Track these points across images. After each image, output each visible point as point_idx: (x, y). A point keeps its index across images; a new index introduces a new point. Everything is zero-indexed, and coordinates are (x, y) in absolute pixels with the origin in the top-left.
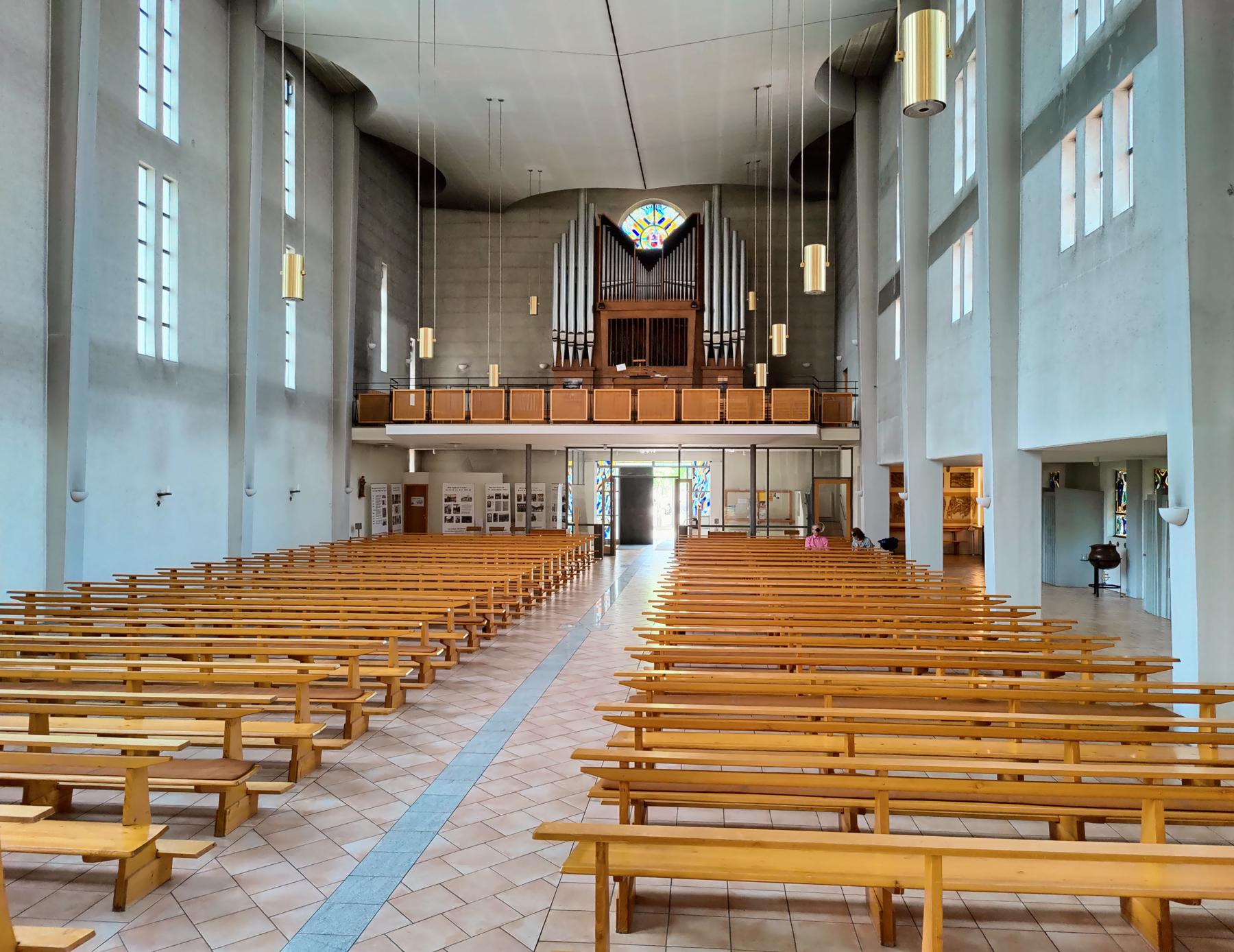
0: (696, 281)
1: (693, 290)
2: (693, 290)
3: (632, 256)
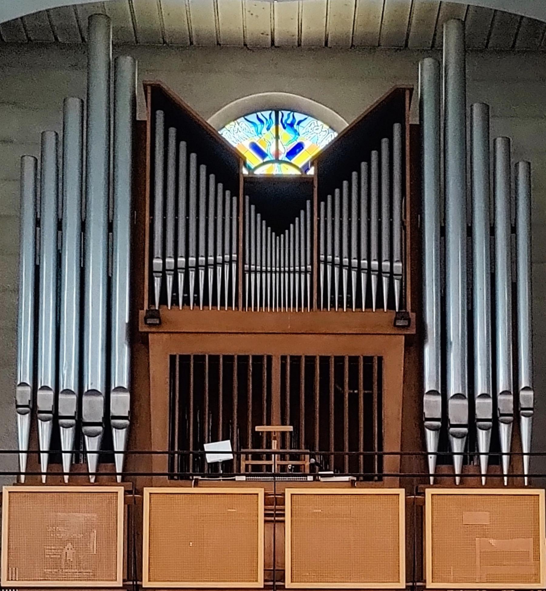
1: (397, 284)
2: (397, 284)
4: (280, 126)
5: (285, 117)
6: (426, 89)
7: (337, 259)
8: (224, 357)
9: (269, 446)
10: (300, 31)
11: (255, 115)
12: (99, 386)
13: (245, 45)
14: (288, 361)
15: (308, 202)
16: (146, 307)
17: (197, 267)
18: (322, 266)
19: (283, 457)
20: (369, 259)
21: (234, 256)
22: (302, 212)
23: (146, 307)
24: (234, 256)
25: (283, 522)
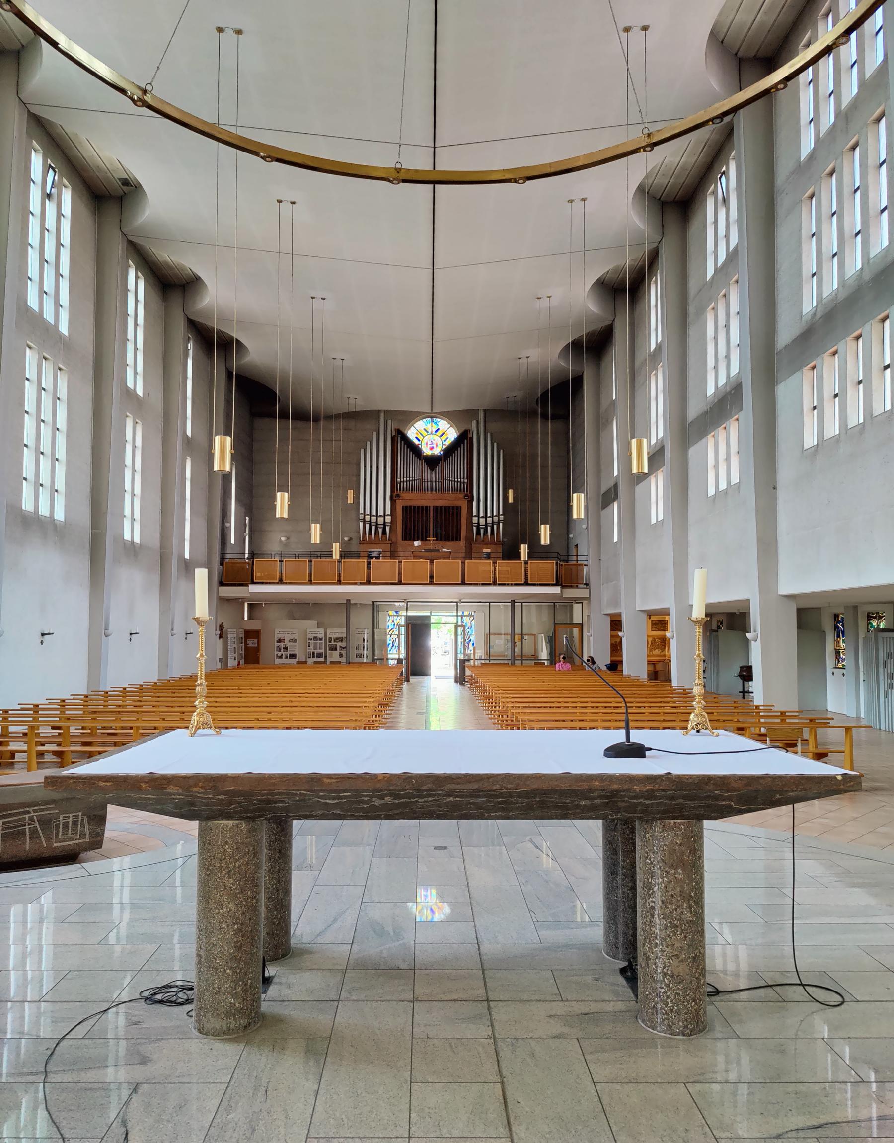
0: (467, 479)
1: (465, 486)
2: (465, 486)
3: (420, 460)
12: (382, 514)
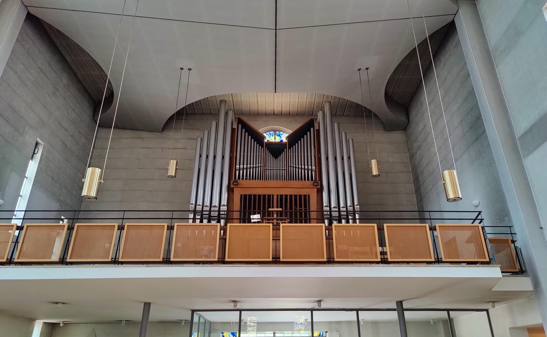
1: (313, 173)
2: (313, 173)
3: (262, 147)
4: (276, 135)
5: (277, 133)
6: (320, 119)
7: (294, 166)
8: (258, 195)
9: (273, 216)
10: (282, 111)
11: (268, 133)
12: (217, 205)
13: (266, 114)
14: (279, 197)
15: (285, 149)
16: (233, 179)
17: (250, 168)
18: (290, 168)
19: (277, 220)
20: (304, 166)
21: (262, 165)
22: (283, 152)
23: (233, 179)
24: (262, 165)
25: (280, 239)
